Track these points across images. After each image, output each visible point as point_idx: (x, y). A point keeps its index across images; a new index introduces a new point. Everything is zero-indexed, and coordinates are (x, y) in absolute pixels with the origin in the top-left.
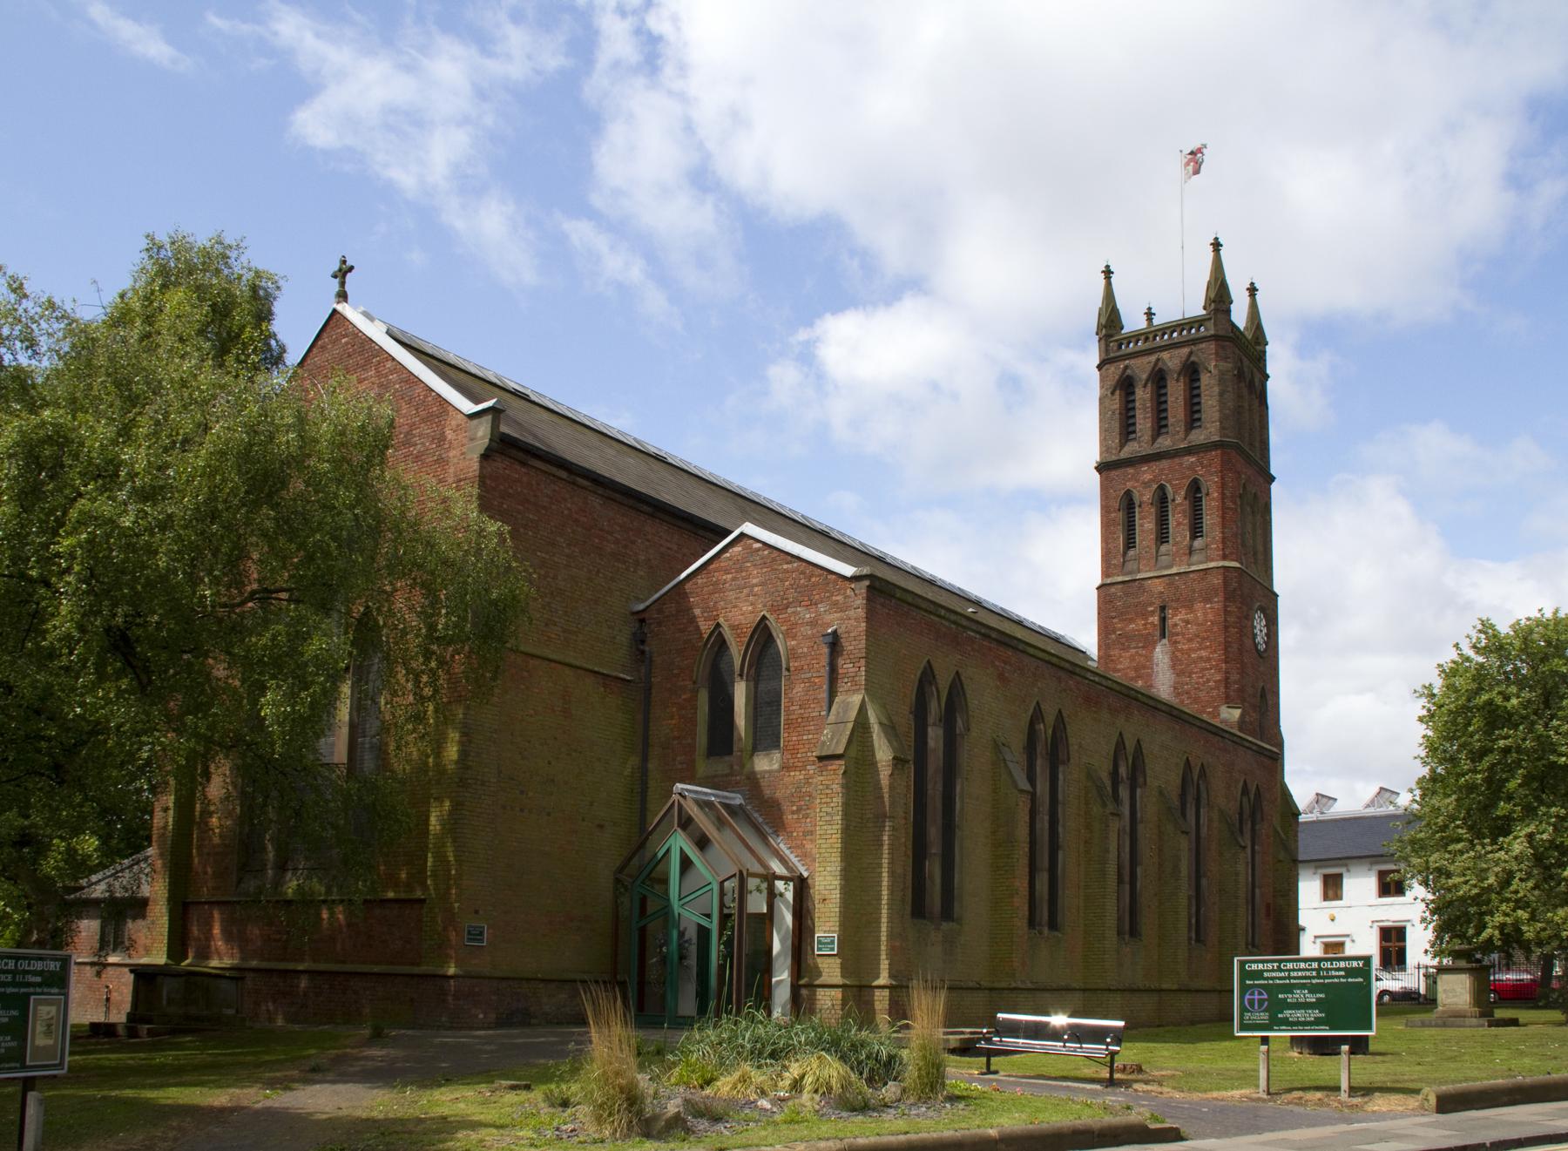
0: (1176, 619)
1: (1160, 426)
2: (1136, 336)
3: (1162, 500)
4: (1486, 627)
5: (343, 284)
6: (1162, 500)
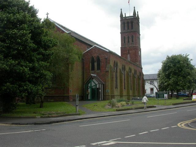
0: (130, 52)
1: (128, 28)
2: (124, 18)
3: (128, 38)
4: (168, 56)
5: (47, 15)
6: (128, 38)
